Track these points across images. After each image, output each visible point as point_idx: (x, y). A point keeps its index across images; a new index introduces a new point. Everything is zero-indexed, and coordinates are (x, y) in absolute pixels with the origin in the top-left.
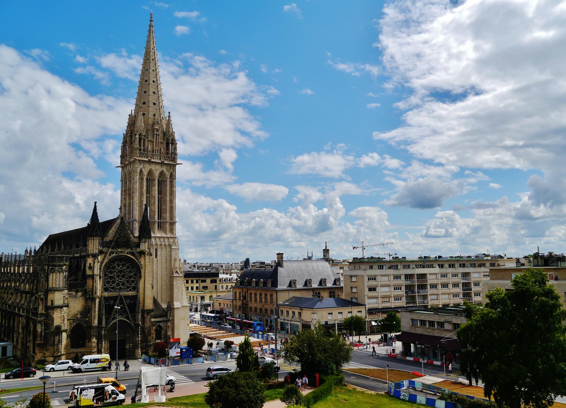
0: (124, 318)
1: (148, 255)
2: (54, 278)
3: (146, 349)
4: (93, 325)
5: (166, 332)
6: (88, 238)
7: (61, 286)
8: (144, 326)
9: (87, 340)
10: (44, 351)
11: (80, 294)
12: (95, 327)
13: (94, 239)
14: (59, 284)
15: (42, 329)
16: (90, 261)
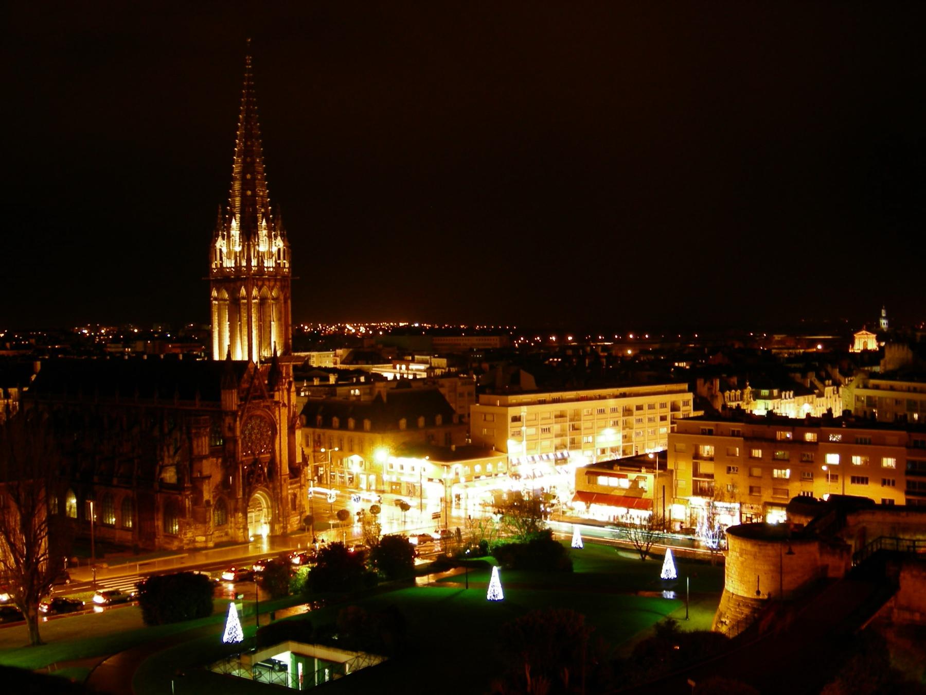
0: (264, 486)
1: (283, 406)
2: (200, 444)
3: (285, 523)
4: (239, 497)
5: (300, 501)
6: (222, 391)
7: (207, 453)
8: (282, 495)
9: (229, 515)
10: (193, 530)
11: (220, 460)
12: (240, 498)
13: (232, 393)
14: (206, 451)
15: (189, 505)
16: (228, 420)
